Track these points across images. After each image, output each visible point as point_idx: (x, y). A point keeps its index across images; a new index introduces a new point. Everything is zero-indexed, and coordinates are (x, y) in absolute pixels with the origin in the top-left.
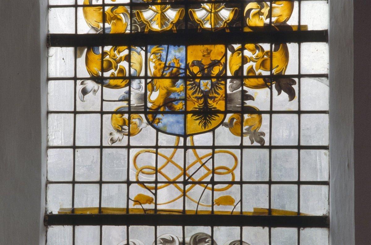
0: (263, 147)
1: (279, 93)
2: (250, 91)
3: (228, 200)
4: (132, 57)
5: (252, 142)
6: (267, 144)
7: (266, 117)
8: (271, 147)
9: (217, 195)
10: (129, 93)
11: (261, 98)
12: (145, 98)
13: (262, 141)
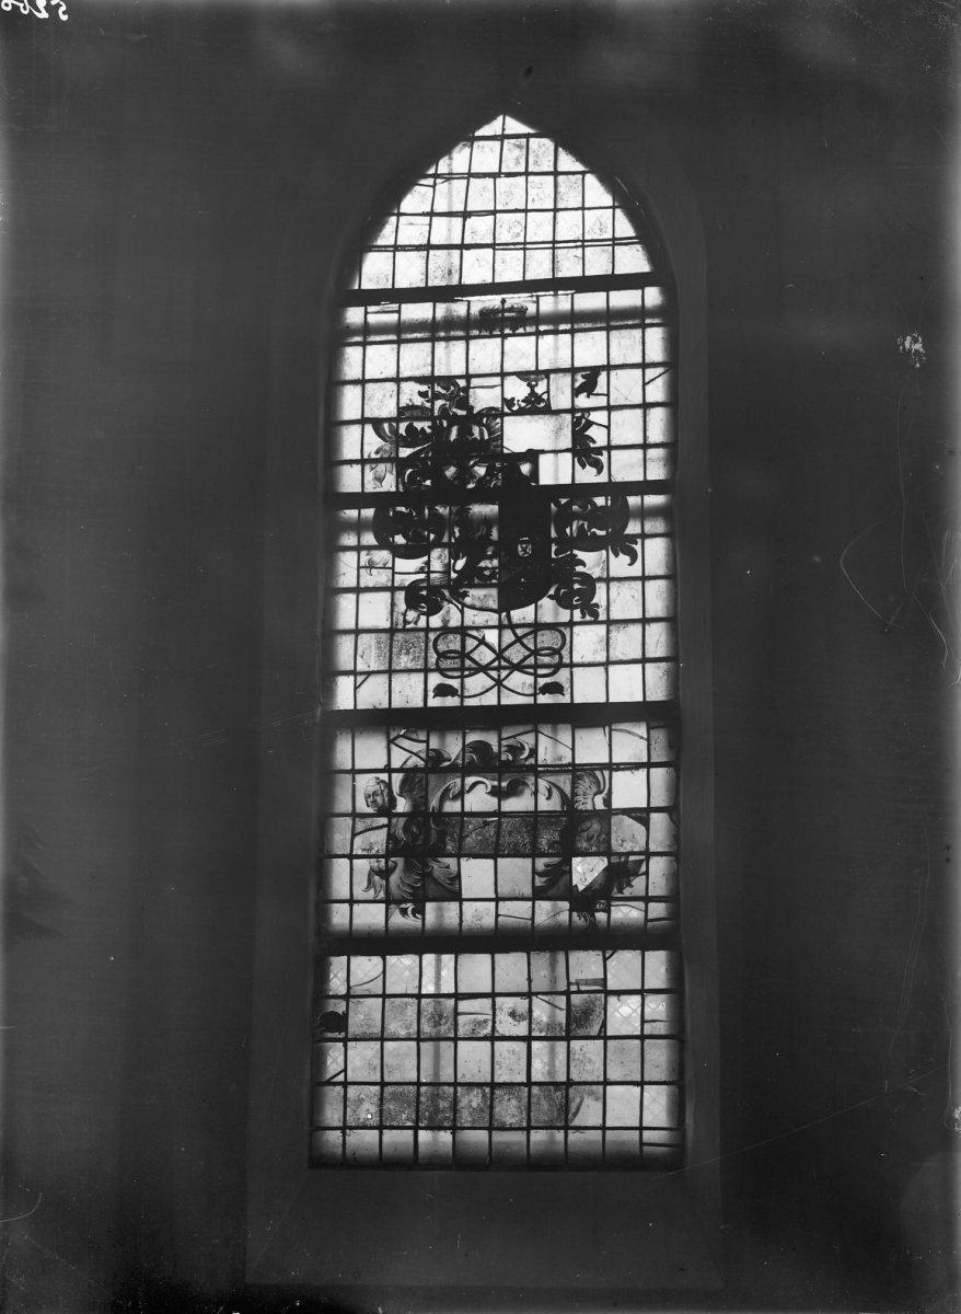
0: (596, 622)
1: (617, 555)
2: (581, 555)
3: (556, 688)
4: (432, 563)
5: (584, 617)
6: (602, 617)
7: (601, 588)
8: (609, 623)
9: (542, 682)
10: (428, 563)
11: (591, 562)
12: (448, 568)
13: (596, 615)
